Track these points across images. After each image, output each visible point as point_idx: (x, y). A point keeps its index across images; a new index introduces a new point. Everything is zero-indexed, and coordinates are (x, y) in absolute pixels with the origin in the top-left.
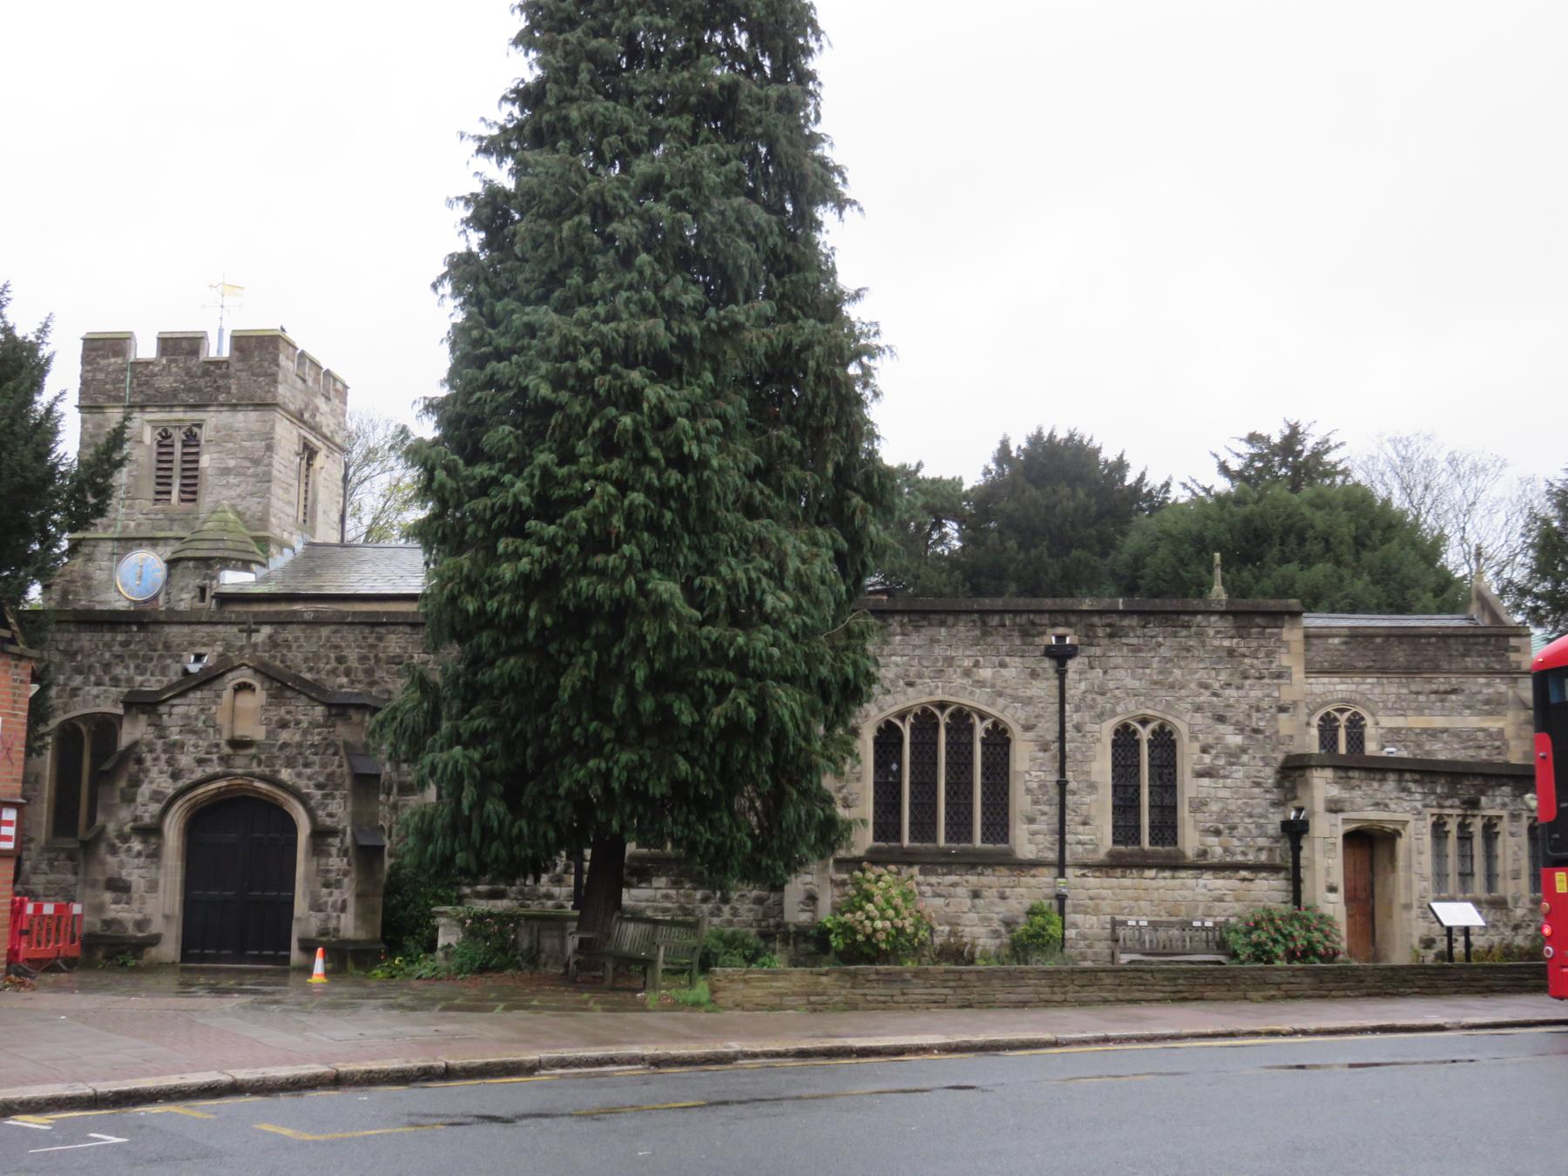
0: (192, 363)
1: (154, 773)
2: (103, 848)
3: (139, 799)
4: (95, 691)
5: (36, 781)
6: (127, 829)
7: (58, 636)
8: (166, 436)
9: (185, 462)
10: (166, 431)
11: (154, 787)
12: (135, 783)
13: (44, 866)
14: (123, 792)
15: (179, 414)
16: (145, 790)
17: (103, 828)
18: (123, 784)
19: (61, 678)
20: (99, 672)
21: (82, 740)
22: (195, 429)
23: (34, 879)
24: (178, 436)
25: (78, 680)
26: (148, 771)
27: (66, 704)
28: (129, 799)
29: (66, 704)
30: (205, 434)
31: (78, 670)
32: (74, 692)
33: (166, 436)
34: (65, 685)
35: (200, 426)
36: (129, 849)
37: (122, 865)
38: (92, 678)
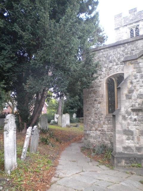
0: (135, 13)
1: (138, 88)
2: (120, 118)
3: (133, 98)
4: (116, 67)
5: (102, 97)
6: (129, 110)
7: (104, 53)
8: (132, 30)
9: (136, 34)
10: (131, 29)
11: (138, 92)
12: (131, 91)
13: (106, 122)
14: (127, 96)
15: (134, 24)
16: (135, 94)
17: (120, 109)
18: (125, 91)
19: (106, 65)
20: (117, 61)
21: (114, 83)
22: (138, 27)
23: (104, 126)
24: (134, 29)
25: (111, 64)
26: (135, 87)
27: (108, 73)
28: (129, 97)
29: (108, 73)
30: (139, 27)
31: (111, 62)
32: (110, 69)
33: (132, 30)
34: (108, 67)
35: (138, 26)
36: (131, 118)
37: (129, 124)
38: (115, 63)
